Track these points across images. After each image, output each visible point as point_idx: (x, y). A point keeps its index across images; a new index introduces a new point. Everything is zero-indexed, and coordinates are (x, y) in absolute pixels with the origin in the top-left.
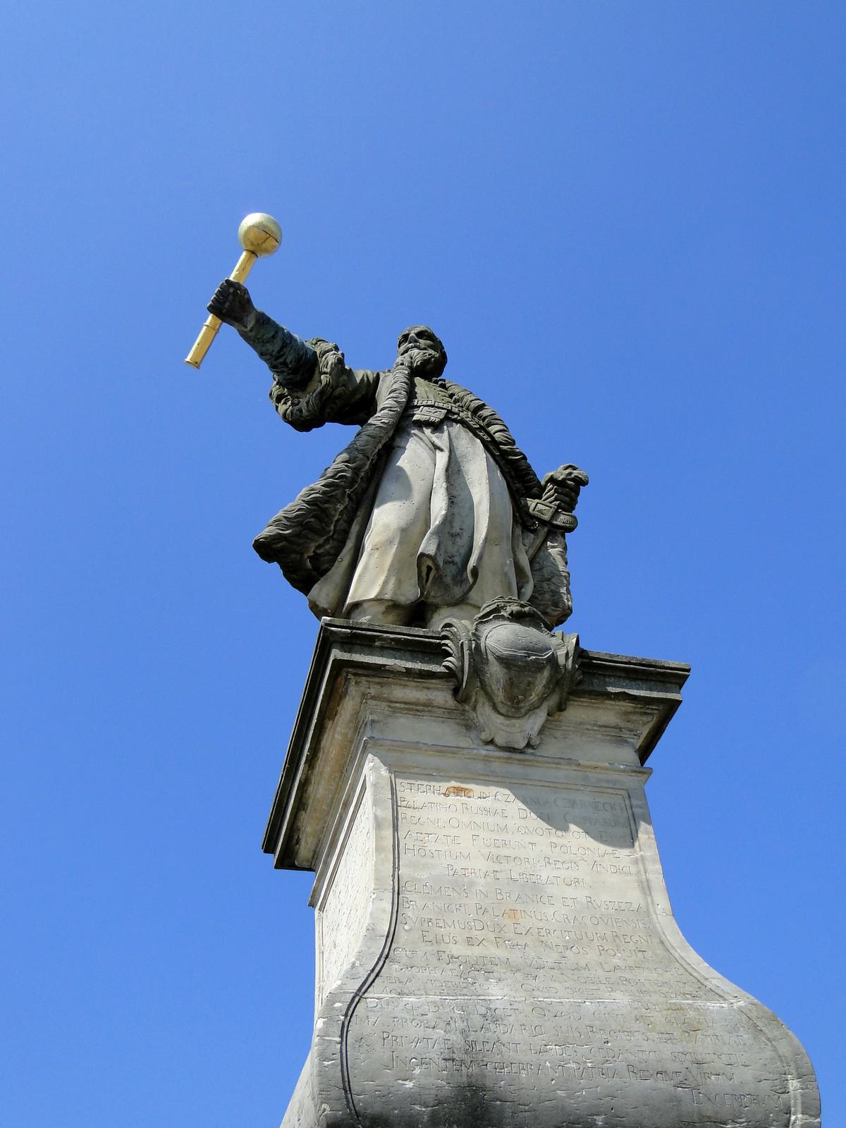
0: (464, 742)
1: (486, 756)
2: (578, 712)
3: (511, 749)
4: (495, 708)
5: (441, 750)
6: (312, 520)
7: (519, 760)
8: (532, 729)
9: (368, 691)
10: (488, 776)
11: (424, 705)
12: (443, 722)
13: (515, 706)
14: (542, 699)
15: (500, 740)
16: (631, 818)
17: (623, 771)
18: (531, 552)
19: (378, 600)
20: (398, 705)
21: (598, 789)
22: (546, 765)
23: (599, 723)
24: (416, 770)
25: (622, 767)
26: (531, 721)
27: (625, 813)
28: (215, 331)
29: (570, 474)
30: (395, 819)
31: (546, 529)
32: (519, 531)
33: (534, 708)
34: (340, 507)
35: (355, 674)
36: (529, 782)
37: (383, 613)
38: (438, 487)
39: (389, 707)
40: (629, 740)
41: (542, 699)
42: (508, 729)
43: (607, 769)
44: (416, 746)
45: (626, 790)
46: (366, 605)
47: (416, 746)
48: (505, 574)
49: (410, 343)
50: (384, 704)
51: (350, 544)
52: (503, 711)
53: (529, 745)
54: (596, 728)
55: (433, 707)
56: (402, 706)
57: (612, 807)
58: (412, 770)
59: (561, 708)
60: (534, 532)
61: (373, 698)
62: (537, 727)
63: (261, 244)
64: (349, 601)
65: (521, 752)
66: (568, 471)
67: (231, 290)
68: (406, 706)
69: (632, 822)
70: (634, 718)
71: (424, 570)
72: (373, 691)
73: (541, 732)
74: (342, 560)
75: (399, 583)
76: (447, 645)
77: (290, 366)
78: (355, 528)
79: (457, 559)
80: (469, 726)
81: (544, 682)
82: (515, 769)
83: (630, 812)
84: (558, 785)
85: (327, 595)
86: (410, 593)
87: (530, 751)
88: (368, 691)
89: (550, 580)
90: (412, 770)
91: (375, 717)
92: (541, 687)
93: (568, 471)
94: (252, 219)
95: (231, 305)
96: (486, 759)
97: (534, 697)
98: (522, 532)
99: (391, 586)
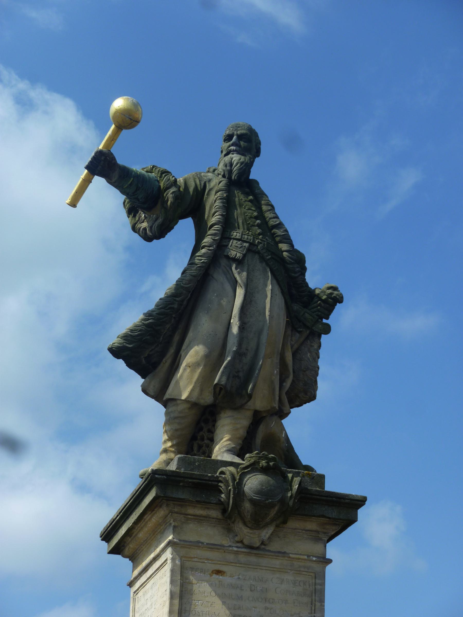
0: (226, 542)
1: (236, 551)
2: (293, 524)
3: (251, 547)
4: (245, 524)
5: (212, 547)
6: (148, 337)
7: (255, 554)
8: (265, 536)
9: (173, 509)
10: (236, 563)
11: (205, 517)
12: (215, 526)
13: (257, 522)
14: (272, 521)
15: (246, 542)
16: (314, 591)
17: (315, 561)
18: (296, 346)
19: (186, 401)
20: (190, 517)
21: (298, 572)
22: (270, 557)
23: (306, 529)
24: (195, 560)
25: (314, 559)
26: (265, 531)
27: (311, 587)
28: (86, 182)
29: (331, 294)
30: (181, 591)
31: (308, 332)
32: (289, 332)
33: (266, 525)
34: (168, 326)
35: (166, 500)
36: (259, 567)
37: (189, 408)
38: (234, 323)
39: (184, 517)
40: (323, 538)
41: (272, 521)
42: (252, 535)
43: (305, 560)
44: (198, 544)
45: (315, 573)
46: (179, 402)
47: (198, 544)
48: (272, 382)
49: (232, 145)
50: (182, 516)
51: (172, 351)
52: (250, 525)
53: (263, 543)
54: (304, 532)
55: (210, 518)
56: (192, 517)
57: (304, 584)
58: (194, 560)
59: (285, 522)
60: (300, 332)
61: (177, 513)
62: (267, 536)
63: (127, 121)
64: (167, 396)
65: (258, 548)
66: (330, 291)
67: (103, 158)
68: (194, 517)
69: (314, 594)
70: (328, 527)
71: (218, 390)
72: (176, 510)
73: (269, 538)
74: (166, 362)
75: (202, 391)
76: (221, 487)
77: (140, 200)
78: (176, 338)
79: (241, 374)
80: (229, 530)
81: (275, 512)
82: (253, 559)
83: (314, 587)
84: (275, 569)
85: (154, 386)
86: (208, 399)
87: (263, 547)
88: (173, 509)
89: (305, 371)
90: (194, 560)
91: (176, 524)
92: (273, 515)
93: (330, 291)
94: (119, 103)
95: (103, 165)
96: (236, 553)
97: (268, 519)
98: (292, 331)
99: (196, 394)
